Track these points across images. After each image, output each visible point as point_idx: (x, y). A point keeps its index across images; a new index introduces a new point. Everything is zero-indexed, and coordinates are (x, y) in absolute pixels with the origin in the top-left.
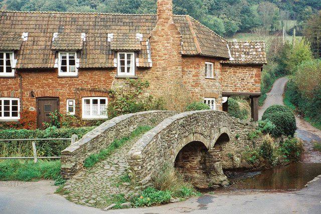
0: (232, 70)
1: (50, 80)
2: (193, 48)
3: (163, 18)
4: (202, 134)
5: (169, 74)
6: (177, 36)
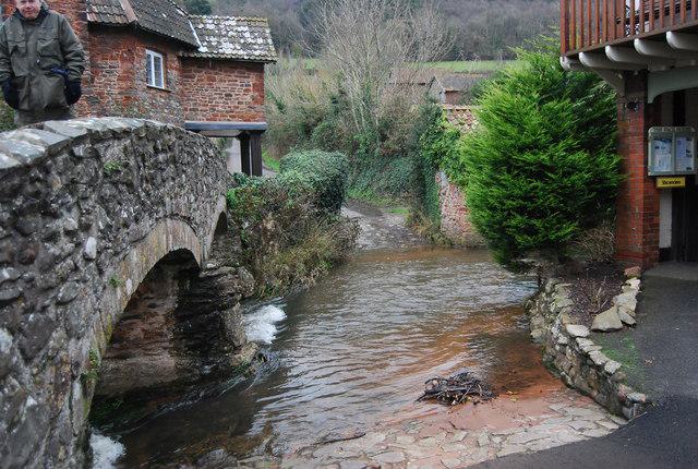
0: (203, 74)
2: (116, 11)
4: (188, 220)
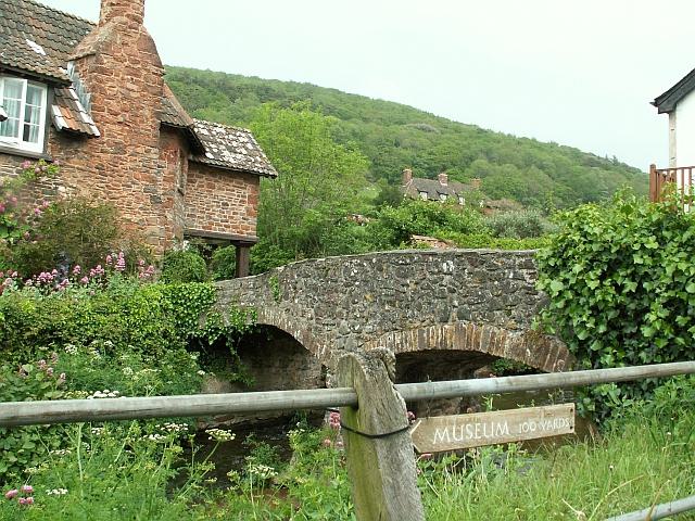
3: (128, 16)
5: (129, 165)
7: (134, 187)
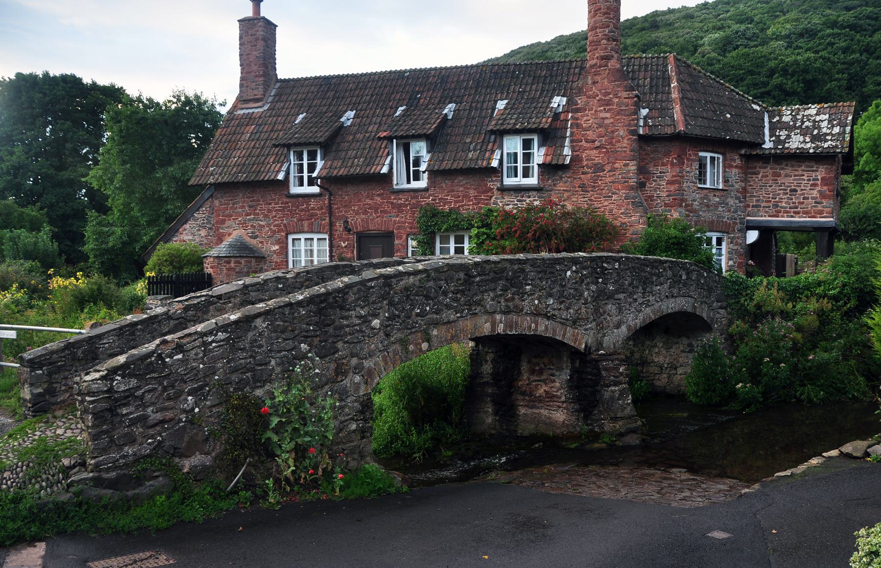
0: (769, 171)
1: (379, 199)
5: (608, 180)
6: (625, 94)
7: (615, 197)
